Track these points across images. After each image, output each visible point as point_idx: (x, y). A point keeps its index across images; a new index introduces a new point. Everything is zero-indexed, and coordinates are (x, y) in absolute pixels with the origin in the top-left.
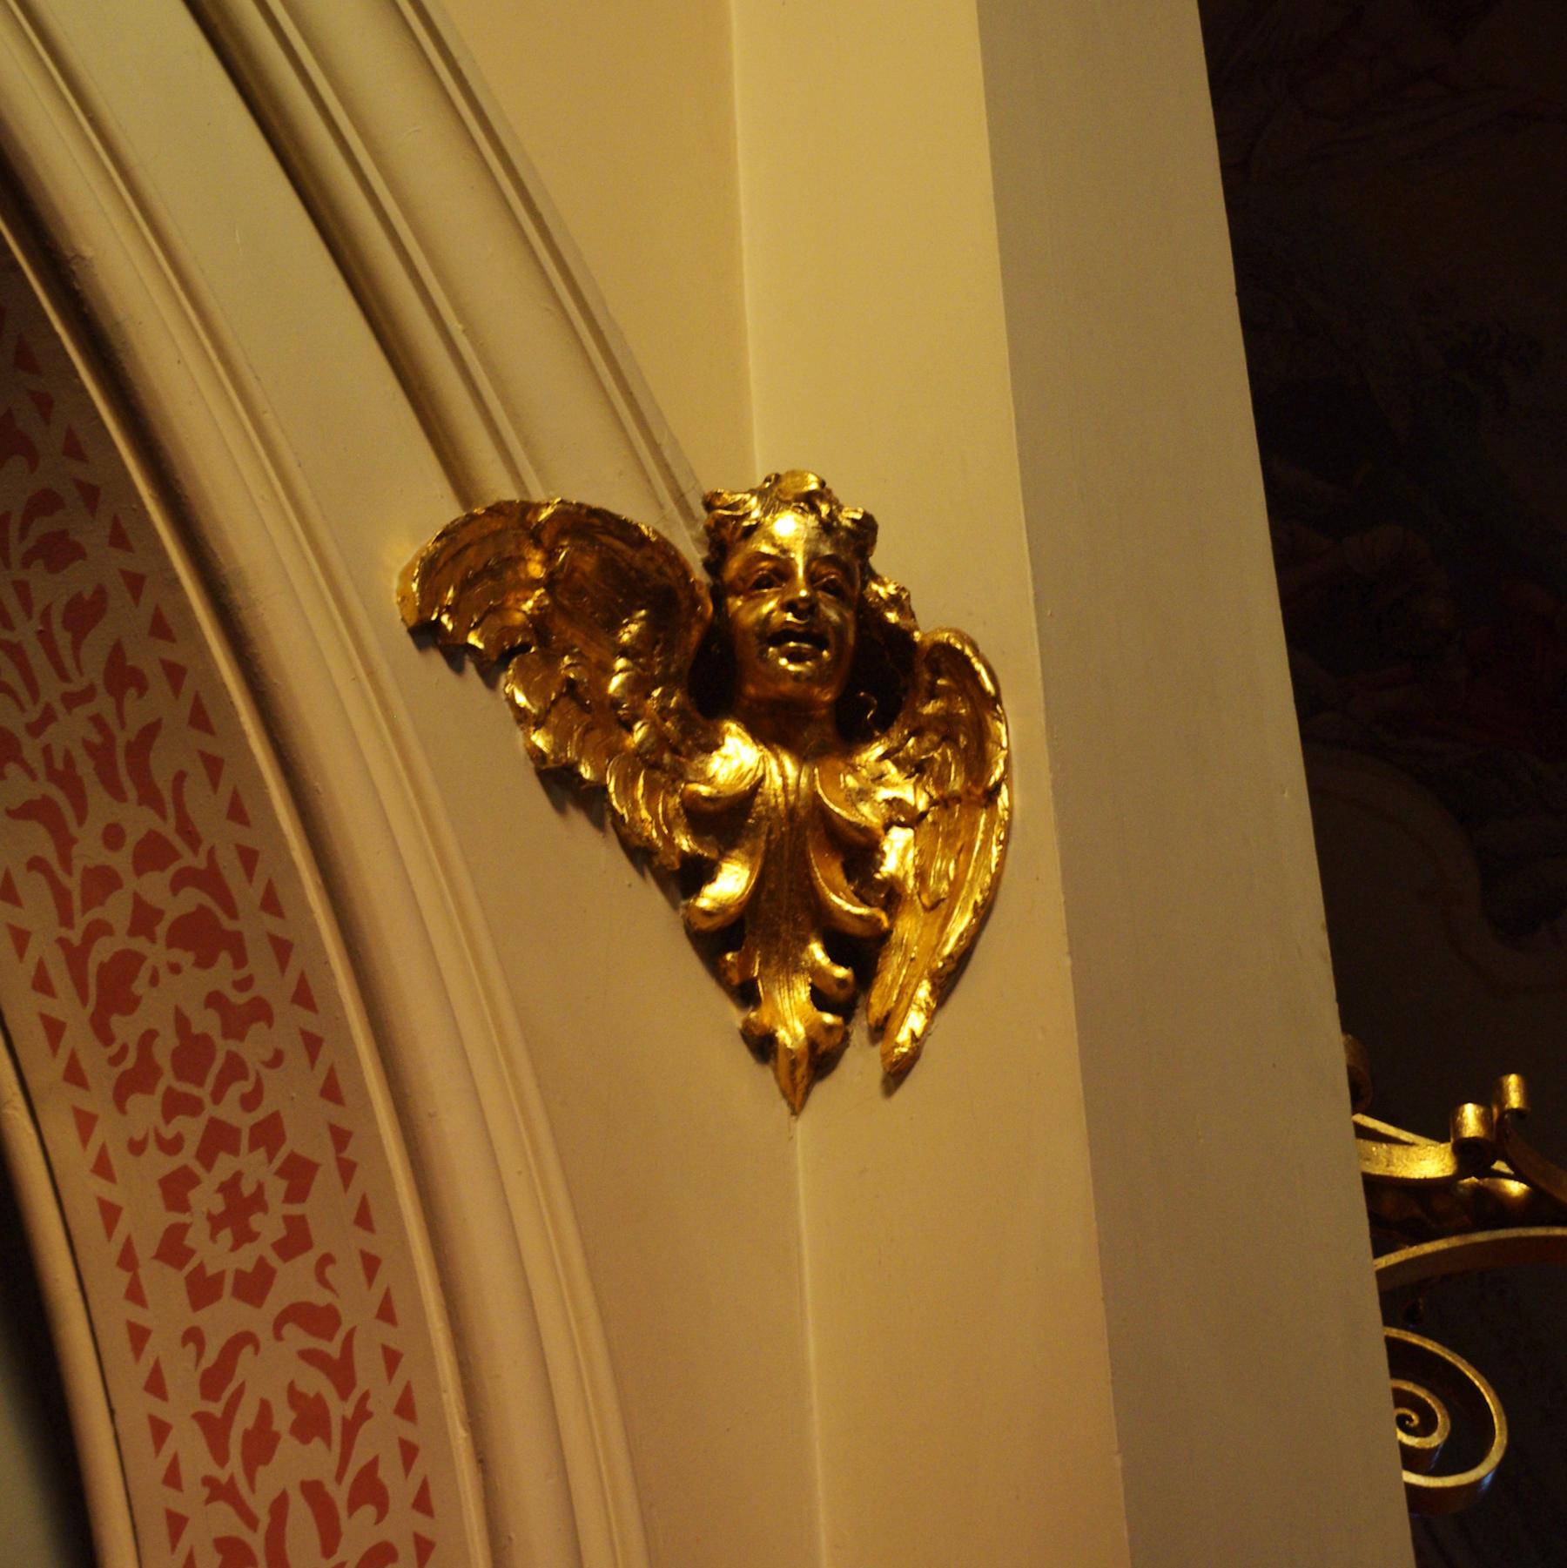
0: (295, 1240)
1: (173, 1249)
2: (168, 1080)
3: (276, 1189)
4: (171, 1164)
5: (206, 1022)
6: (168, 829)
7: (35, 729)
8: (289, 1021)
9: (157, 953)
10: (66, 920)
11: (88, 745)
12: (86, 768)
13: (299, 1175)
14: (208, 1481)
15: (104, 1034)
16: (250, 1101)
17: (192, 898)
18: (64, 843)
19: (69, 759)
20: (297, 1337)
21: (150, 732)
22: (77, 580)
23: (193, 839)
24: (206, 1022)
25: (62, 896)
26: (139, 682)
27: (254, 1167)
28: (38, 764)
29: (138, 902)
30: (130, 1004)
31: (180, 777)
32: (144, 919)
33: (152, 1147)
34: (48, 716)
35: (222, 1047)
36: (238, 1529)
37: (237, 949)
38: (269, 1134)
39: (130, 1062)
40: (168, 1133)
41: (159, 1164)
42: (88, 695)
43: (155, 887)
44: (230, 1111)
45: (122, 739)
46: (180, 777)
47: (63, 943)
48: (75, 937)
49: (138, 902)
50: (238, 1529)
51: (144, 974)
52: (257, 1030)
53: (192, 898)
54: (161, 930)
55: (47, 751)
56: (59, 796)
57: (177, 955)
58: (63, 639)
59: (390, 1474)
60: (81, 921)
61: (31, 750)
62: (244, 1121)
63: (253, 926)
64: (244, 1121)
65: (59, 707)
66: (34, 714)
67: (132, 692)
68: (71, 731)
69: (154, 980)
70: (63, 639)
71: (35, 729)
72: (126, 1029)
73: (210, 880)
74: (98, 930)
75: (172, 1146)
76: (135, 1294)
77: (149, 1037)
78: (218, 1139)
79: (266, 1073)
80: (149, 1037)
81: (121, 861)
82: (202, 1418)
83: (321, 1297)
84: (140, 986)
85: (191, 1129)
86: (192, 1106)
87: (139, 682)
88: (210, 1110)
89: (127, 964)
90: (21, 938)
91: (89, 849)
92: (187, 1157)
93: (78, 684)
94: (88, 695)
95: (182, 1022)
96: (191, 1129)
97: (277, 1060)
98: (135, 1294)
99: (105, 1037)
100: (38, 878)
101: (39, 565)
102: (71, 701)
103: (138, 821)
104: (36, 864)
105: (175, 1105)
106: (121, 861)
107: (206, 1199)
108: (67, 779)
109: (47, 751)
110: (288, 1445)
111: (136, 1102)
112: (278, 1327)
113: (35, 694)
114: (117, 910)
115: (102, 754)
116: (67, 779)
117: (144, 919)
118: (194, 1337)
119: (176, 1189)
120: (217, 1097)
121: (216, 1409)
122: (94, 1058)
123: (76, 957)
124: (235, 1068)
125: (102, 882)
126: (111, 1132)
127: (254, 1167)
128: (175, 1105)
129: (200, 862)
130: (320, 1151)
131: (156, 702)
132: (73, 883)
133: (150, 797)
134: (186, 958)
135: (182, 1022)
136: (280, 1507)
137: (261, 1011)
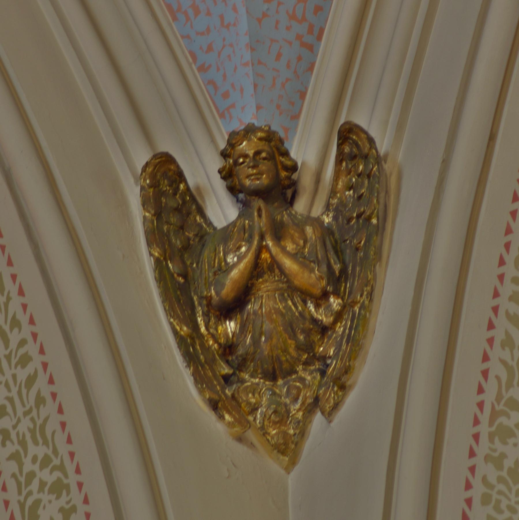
9: (45, 497)
10: (20, 493)
11: (29, 429)
18: (21, 465)
19: (24, 435)
29: (41, 480)
45: (39, 422)
48: (22, 498)
49: (41, 480)
53: (57, 474)
55: (18, 434)
58: (24, 391)
60: (24, 493)
66: (15, 421)
69: (44, 507)
70: (24, 391)
71: (14, 427)
74: (30, 493)
81: (36, 468)
90: (7, 503)
91: (28, 467)
100: (13, 480)
101: (19, 367)
102: (26, 414)
113: (15, 414)
114: (35, 485)
117: (42, 484)
125: (31, 476)
132: (22, 480)
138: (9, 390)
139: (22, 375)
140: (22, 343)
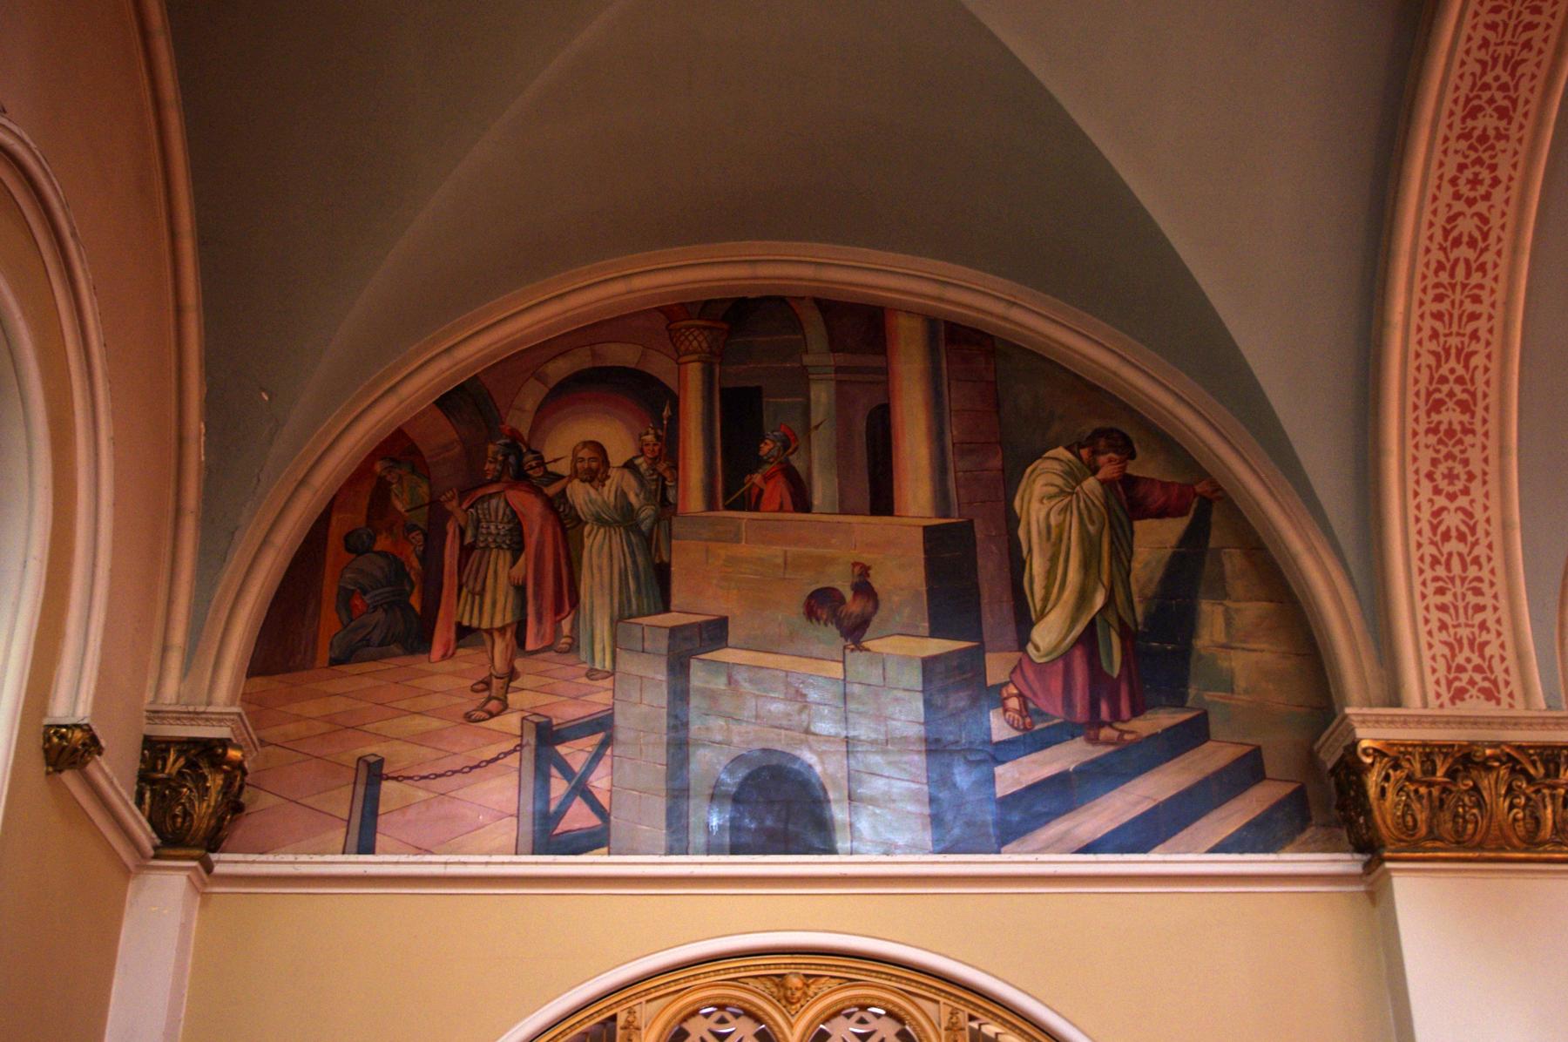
0: (1466, 491)
1: (1430, 476)
2: (1441, 434)
3: (1463, 477)
4: (1435, 455)
5: (1457, 427)
6: (1467, 377)
9: (1450, 404)
10: (1431, 382)
11: (1457, 348)
12: (1453, 351)
13: (1471, 477)
15: (1428, 414)
16: (1463, 452)
17: (1465, 396)
18: (1439, 366)
20: (1460, 515)
22: (1477, 308)
24: (1457, 427)
26: (1478, 340)
27: (1459, 469)
30: (1439, 412)
32: (1451, 394)
34: (1450, 334)
35: (1459, 435)
37: (1473, 416)
38: (1466, 462)
39: (1433, 425)
41: (1431, 453)
42: (1464, 335)
43: (1457, 389)
48: (1431, 389)
52: (1470, 436)
53: (1465, 396)
57: (1456, 407)
59: (1483, 560)
60: (1434, 386)
62: (1459, 456)
63: (1480, 412)
64: (1459, 456)
66: (1447, 331)
67: (1474, 342)
68: (1454, 341)
71: (1446, 335)
73: (1473, 395)
74: (1438, 390)
75: (1438, 451)
78: (1450, 456)
81: (1452, 378)
82: (1431, 523)
83: (1468, 507)
84: (1443, 409)
86: (1446, 445)
87: (1478, 340)
92: (1440, 456)
94: (1464, 335)
95: (1450, 423)
96: (1444, 450)
103: (1460, 371)
105: (1440, 442)
106: (1452, 378)
107: (1442, 468)
108: (1447, 351)
109: (1446, 342)
112: (1457, 509)
115: (1459, 351)
117: (1451, 394)
118: (1431, 501)
119: (1435, 462)
120: (1454, 445)
123: (1429, 394)
124: (1460, 442)
125: (1443, 380)
127: (1459, 469)
128: (1440, 442)
129: (1472, 389)
131: (1480, 347)
134: (1458, 410)
135: (1450, 423)
139: (1469, 307)
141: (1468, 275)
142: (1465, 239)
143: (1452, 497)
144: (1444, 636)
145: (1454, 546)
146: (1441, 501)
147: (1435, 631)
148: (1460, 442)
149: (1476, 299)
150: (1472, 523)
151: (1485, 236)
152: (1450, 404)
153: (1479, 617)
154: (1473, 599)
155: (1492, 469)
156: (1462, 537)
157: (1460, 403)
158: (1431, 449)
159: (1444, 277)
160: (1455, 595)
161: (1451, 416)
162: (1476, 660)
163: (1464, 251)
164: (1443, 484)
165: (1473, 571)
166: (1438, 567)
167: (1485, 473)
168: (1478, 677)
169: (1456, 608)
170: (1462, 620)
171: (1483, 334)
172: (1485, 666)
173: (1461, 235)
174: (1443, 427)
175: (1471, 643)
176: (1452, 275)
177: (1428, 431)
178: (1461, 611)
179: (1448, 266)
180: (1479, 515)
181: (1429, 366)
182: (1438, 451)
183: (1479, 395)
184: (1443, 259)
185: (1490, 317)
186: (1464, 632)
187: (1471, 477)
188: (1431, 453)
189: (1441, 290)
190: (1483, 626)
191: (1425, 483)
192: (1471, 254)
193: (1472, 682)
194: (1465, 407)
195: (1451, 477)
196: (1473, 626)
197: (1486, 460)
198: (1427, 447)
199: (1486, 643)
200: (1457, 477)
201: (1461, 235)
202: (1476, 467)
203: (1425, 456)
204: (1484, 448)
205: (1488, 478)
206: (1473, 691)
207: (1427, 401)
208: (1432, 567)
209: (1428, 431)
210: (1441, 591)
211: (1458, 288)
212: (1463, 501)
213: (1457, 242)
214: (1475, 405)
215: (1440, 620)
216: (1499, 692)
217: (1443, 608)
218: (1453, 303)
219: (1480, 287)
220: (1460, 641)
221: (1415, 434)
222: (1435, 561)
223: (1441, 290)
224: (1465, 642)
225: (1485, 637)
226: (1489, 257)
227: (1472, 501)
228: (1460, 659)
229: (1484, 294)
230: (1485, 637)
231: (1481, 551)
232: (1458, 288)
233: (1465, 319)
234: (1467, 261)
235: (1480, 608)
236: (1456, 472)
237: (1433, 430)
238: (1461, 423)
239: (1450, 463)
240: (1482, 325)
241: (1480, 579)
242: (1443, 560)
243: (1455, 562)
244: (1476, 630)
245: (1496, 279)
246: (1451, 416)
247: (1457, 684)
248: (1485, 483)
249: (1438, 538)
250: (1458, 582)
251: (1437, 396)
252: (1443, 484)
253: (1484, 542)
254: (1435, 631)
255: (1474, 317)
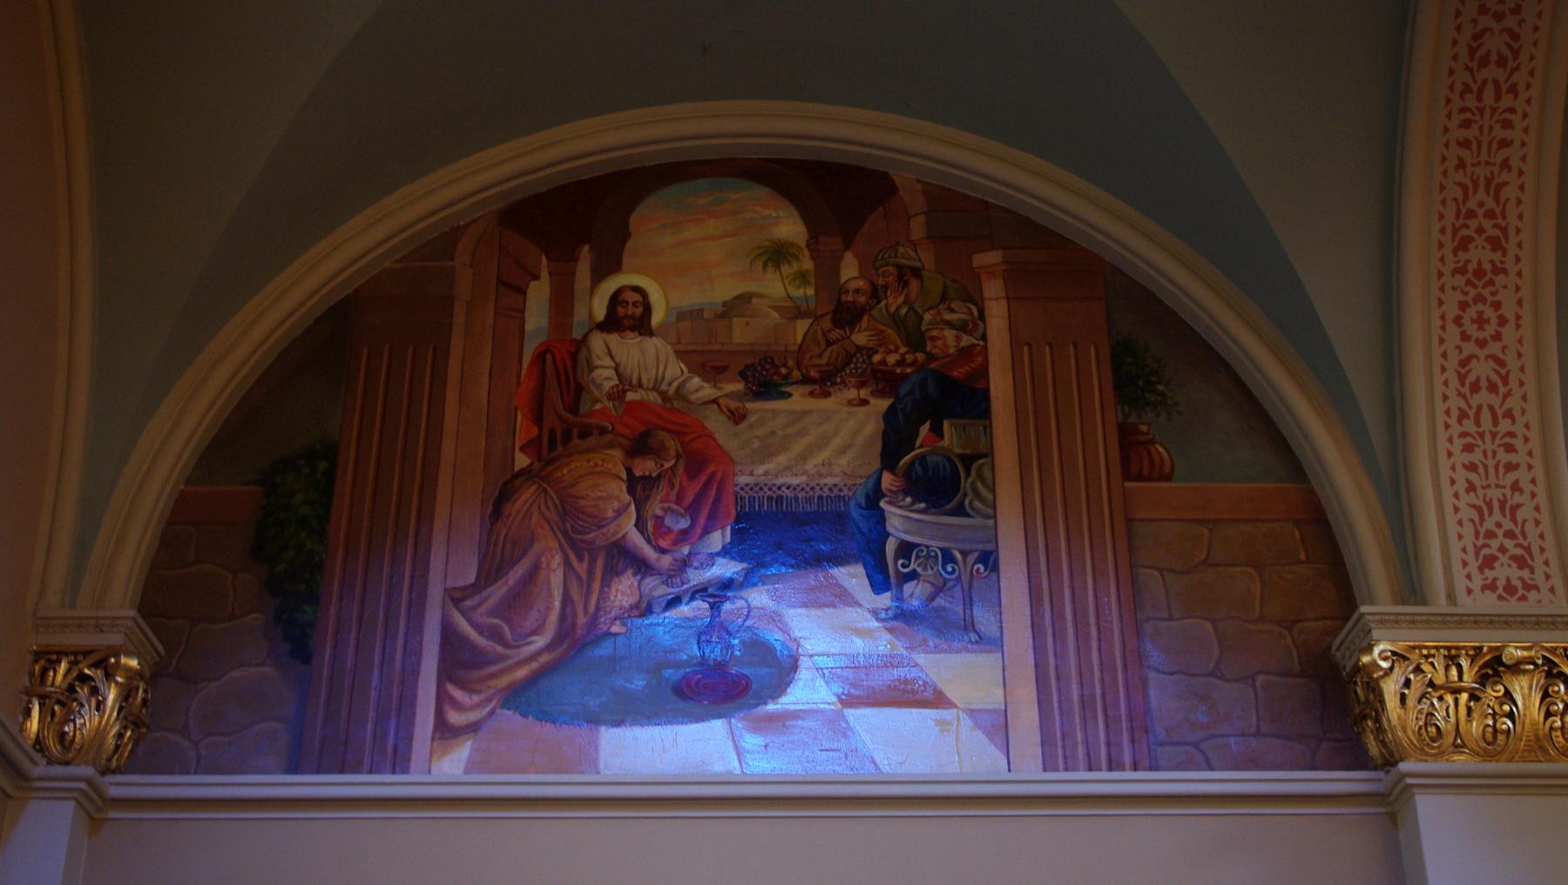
0: (1497, 337)
1: (1458, 321)
2: (1470, 275)
3: (1494, 321)
4: (1463, 298)
5: (1487, 267)
6: (1498, 211)
7: (1473, 165)
8: (1512, 279)
10: (1457, 217)
11: (1486, 178)
13: (1503, 321)
14: (1457, 390)
15: (1455, 253)
16: (1493, 294)
17: (1497, 232)
19: (1478, 178)
21: (1505, 184)
23: (1504, 217)
24: (1487, 267)
25: (1458, 212)
26: (1510, 170)
27: (1489, 313)
28: (1469, 174)
30: (1466, 250)
31: (1508, 200)
32: (1480, 230)
33: (1459, 290)
34: (1479, 164)
35: (1490, 275)
36: (1465, 406)
37: (1504, 254)
38: (1497, 306)
39: (1460, 265)
40: (1466, 289)
41: (1459, 296)
42: (1494, 165)
43: (1487, 224)
44: (1486, 293)
45: (1497, 180)
46: (1508, 200)
47: (1453, 224)
48: (1458, 224)
50: (1465, 406)
51: (1474, 244)
52: (1502, 276)
53: (1497, 232)
54: (1484, 236)
56: (1470, 185)
57: (1486, 245)
59: (1517, 412)
60: (1461, 221)
61: (1469, 169)
62: (1490, 298)
63: (1511, 248)
64: (1490, 298)
65: (1483, 163)
66: (1475, 161)
67: (1505, 171)
68: (1483, 172)
69: (1476, 247)
70: (1495, 146)
71: (1473, 165)
72: (1462, 256)
73: (1504, 230)
74: (1466, 226)
75: (1466, 294)
76: (1443, 328)
77: (1468, 262)
78: (1480, 299)
79: (1501, 289)
80: (1468, 262)
81: (1480, 212)
82: (1458, 373)
84: (1471, 246)
85: (1473, 292)
86: (1475, 286)
87: (1510, 170)
88: (1480, 289)
89: (1469, 239)
92: (1469, 298)
93: (1492, 161)
94: (1494, 165)
95: (1480, 263)
96: (1473, 292)
97: (1505, 287)
98: (1443, 328)
99: (1455, 254)
103: (1490, 203)
104: (1455, 200)
105: (1469, 283)
106: (1480, 212)
107: (1471, 312)
108: (1475, 183)
110: (1484, 393)
111: (1458, 276)
112: (1487, 357)
114: (1473, 224)
115: (1489, 181)
116: (1475, 183)
117: (1480, 230)
118: (1459, 348)
119: (1463, 306)
120: (1484, 287)
121: (1463, 371)
122: (1450, 258)
123: (1455, 231)
124: (1491, 283)
125: (1471, 214)
126: (1448, 280)
127: (1489, 313)
128: (1469, 283)
129: (1503, 224)
130: (1512, 319)
133: (1497, 199)
134: (1488, 247)
135: (1480, 263)
136: (1480, 407)
137: (1505, 272)
138: (1481, 133)
139: (1499, 133)
140: (1512, 110)
141: (1498, 97)
142: (1494, 58)
143: (1482, 344)
144: (1472, 498)
145: (1484, 397)
146: (1469, 348)
147: (1462, 492)
148: (1491, 283)
149: (1507, 124)
150: (1503, 372)
151: (1516, 54)
152: (1480, 240)
153: (1511, 477)
154: (1504, 457)
155: (1526, 312)
156: (1493, 388)
157: (1489, 239)
158: (1459, 292)
159: (1471, 101)
160: (1485, 453)
161: (1479, 254)
162: (1508, 524)
163: (1492, 72)
164: (1472, 329)
165: (1505, 426)
166: (1465, 422)
167: (1518, 317)
168: (1509, 544)
169: (1486, 467)
170: (1492, 480)
171: (1515, 163)
172: (1517, 531)
173: (1489, 53)
174: (1472, 267)
175: (1503, 504)
176: (1479, 98)
177: (1455, 272)
178: (1491, 470)
179: (1475, 88)
180: (1513, 364)
181: (1455, 200)
182: (1466, 294)
183: (1512, 231)
184: (1469, 80)
185: (1523, 144)
186: (1494, 494)
187: (1503, 321)
188: (1459, 296)
189: (1468, 115)
190: (1516, 487)
191: (1451, 327)
192: (1500, 74)
193: (1503, 549)
194: (1495, 244)
195: (1481, 321)
196: (1504, 487)
197: (1520, 303)
198: (1454, 289)
199: (1519, 506)
200: (1488, 321)
201: (1489, 53)
202: (1508, 310)
203: (1453, 299)
204: (1518, 289)
205: (1521, 322)
206: (1504, 559)
207: (1453, 240)
208: (1460, 421)
209: (1455, 272)
210: (1468, 448)
211: (1487, 112)
212: (1495, 348)
213: (1484, 62)
214: (1507, 240)
215: (1468, 481)
216: (1533, 560)
217: (1472, 467)
218: (1481, 129)
219: (1512, 110)
220: (1489, 505)
221: (1440, 275)
222: (1463, 415)
223: (1468, 115)
224: (1496, 504)
225: (1517, 498)
226: (1520, 78)
227: (1504, 347)
228: (1489, 524)
229: (1516, 119)
230: (1517, 498)
231: (1514, 403)
232: (1487, 112)
233: (1495, 146)
234: (1496, 83)
235: (1511, 467)
236: (1486, 316)
237: (1461, 271)
238: (1492, 262)
239: (1480, 307)
240: (1514, 153)
241: (1512, 435)
242: (1471, 413)
243: (1486, 417)
244: (1508, 492)
245: (1528, 102)
246: (1479, 254)
247: (1486, 551)
248: (1518, 327)
249: (1466, 390)
250: (1488, 437)
251: (1464, 232)
252: (1472, 329)
253: (1517, 392)
254: (1462, 492)
255: (1504, 144)
